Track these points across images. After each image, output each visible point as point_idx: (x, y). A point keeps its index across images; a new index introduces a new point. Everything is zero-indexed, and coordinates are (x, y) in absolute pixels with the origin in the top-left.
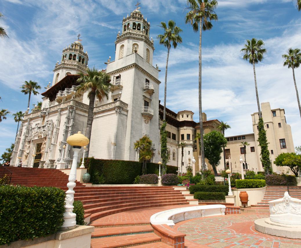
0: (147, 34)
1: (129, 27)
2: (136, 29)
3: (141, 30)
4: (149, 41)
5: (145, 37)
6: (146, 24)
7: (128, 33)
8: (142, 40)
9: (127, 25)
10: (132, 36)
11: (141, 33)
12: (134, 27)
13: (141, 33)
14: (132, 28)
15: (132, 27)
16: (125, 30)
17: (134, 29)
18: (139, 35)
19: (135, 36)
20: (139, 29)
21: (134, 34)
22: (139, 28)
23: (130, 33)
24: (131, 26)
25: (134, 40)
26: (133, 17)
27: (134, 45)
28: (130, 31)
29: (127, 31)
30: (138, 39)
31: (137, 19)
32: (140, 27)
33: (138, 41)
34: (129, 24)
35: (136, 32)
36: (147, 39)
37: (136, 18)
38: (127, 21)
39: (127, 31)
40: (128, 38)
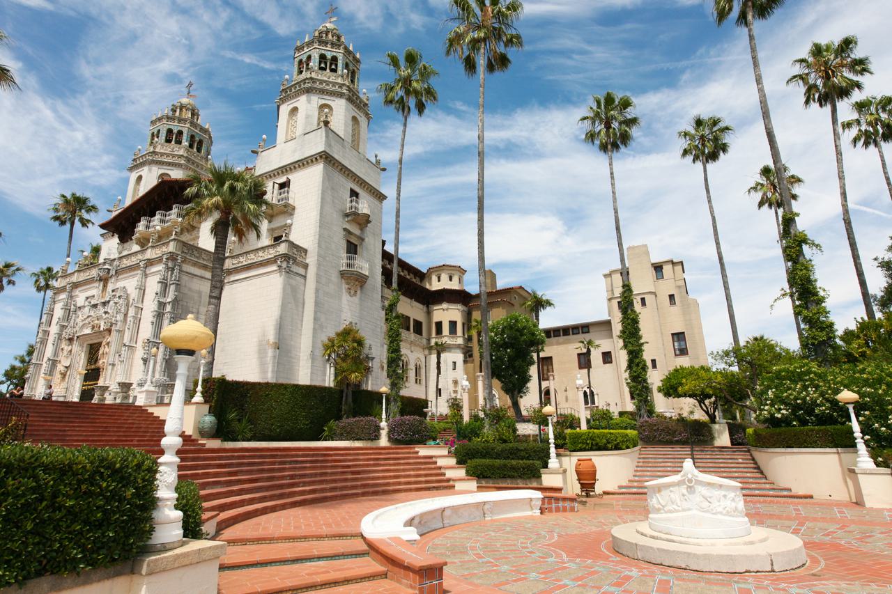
0: (352, 81)
1: (311, 64)
2: (328, 70)
3: (339, 72)
4: (358, 97)
5: (349, 90)
6: (351, 58)
7: (307, 79)
8: (341, 95)
9: (304, 60)
10: (317, 85)
11: (338, 78)
12: (323, 65)
13: (338, 78)
14: (317, 68)
15: (317, 64)
16: (301, 72)
17: (321, 69)
18: (334, 84)
19: (324, 86)
20: (334, 71)
21: (322, 82)
22: (333, 67)
23: (311, 78)
24: (314, 63)
25: (321, 96)
26: (320, 42)
27: (322, 107)
28: (314, 75)
29: (305, 75)
30: (332, 93)
31: (329, 46)
32: (336, 65)
33: (332, 98)
34: (309, 58)
35: (326, 76)
36: (354, 94)
37: (327, 43)
38: (306, 50)
39: (305, 75)
40: (308, 91)
